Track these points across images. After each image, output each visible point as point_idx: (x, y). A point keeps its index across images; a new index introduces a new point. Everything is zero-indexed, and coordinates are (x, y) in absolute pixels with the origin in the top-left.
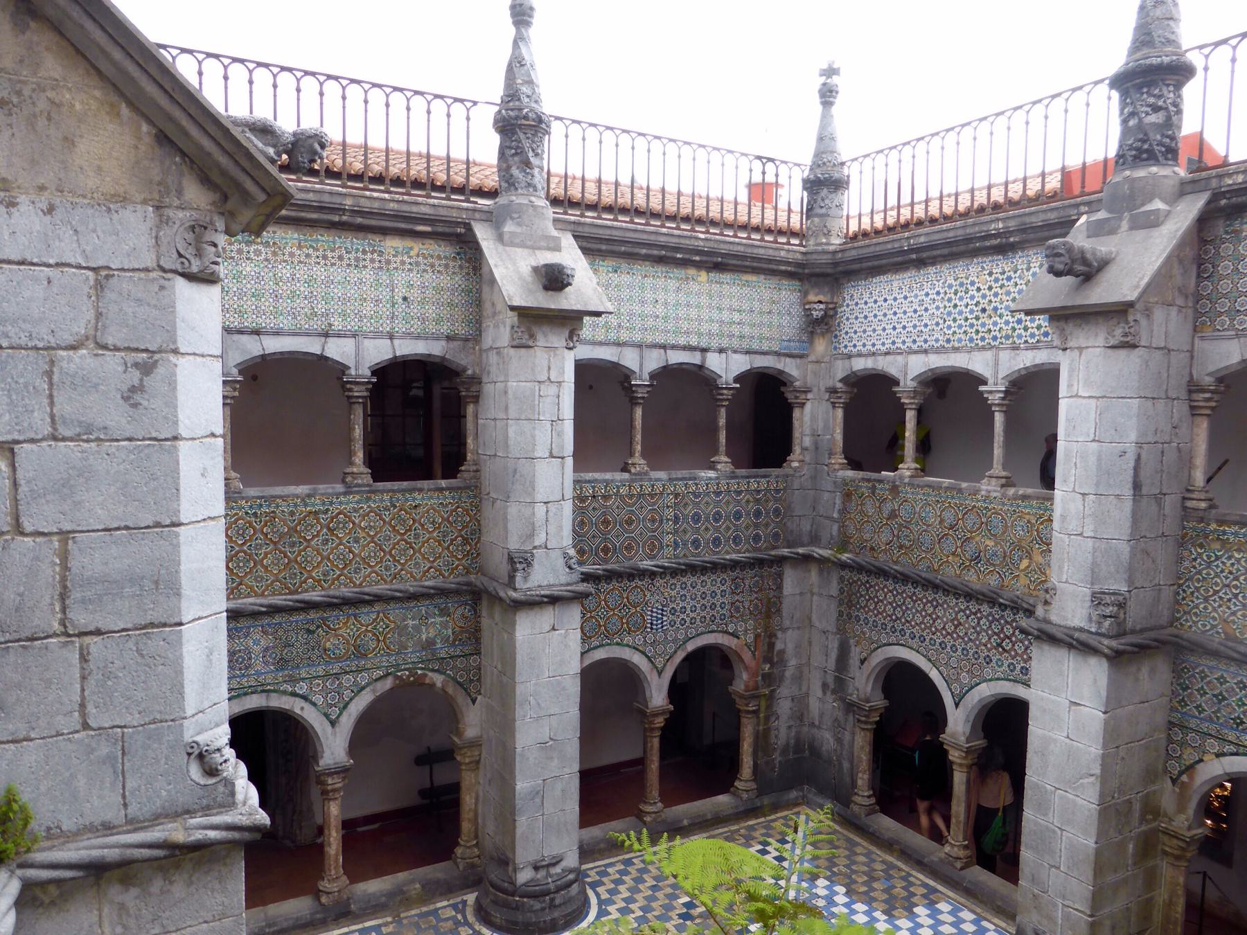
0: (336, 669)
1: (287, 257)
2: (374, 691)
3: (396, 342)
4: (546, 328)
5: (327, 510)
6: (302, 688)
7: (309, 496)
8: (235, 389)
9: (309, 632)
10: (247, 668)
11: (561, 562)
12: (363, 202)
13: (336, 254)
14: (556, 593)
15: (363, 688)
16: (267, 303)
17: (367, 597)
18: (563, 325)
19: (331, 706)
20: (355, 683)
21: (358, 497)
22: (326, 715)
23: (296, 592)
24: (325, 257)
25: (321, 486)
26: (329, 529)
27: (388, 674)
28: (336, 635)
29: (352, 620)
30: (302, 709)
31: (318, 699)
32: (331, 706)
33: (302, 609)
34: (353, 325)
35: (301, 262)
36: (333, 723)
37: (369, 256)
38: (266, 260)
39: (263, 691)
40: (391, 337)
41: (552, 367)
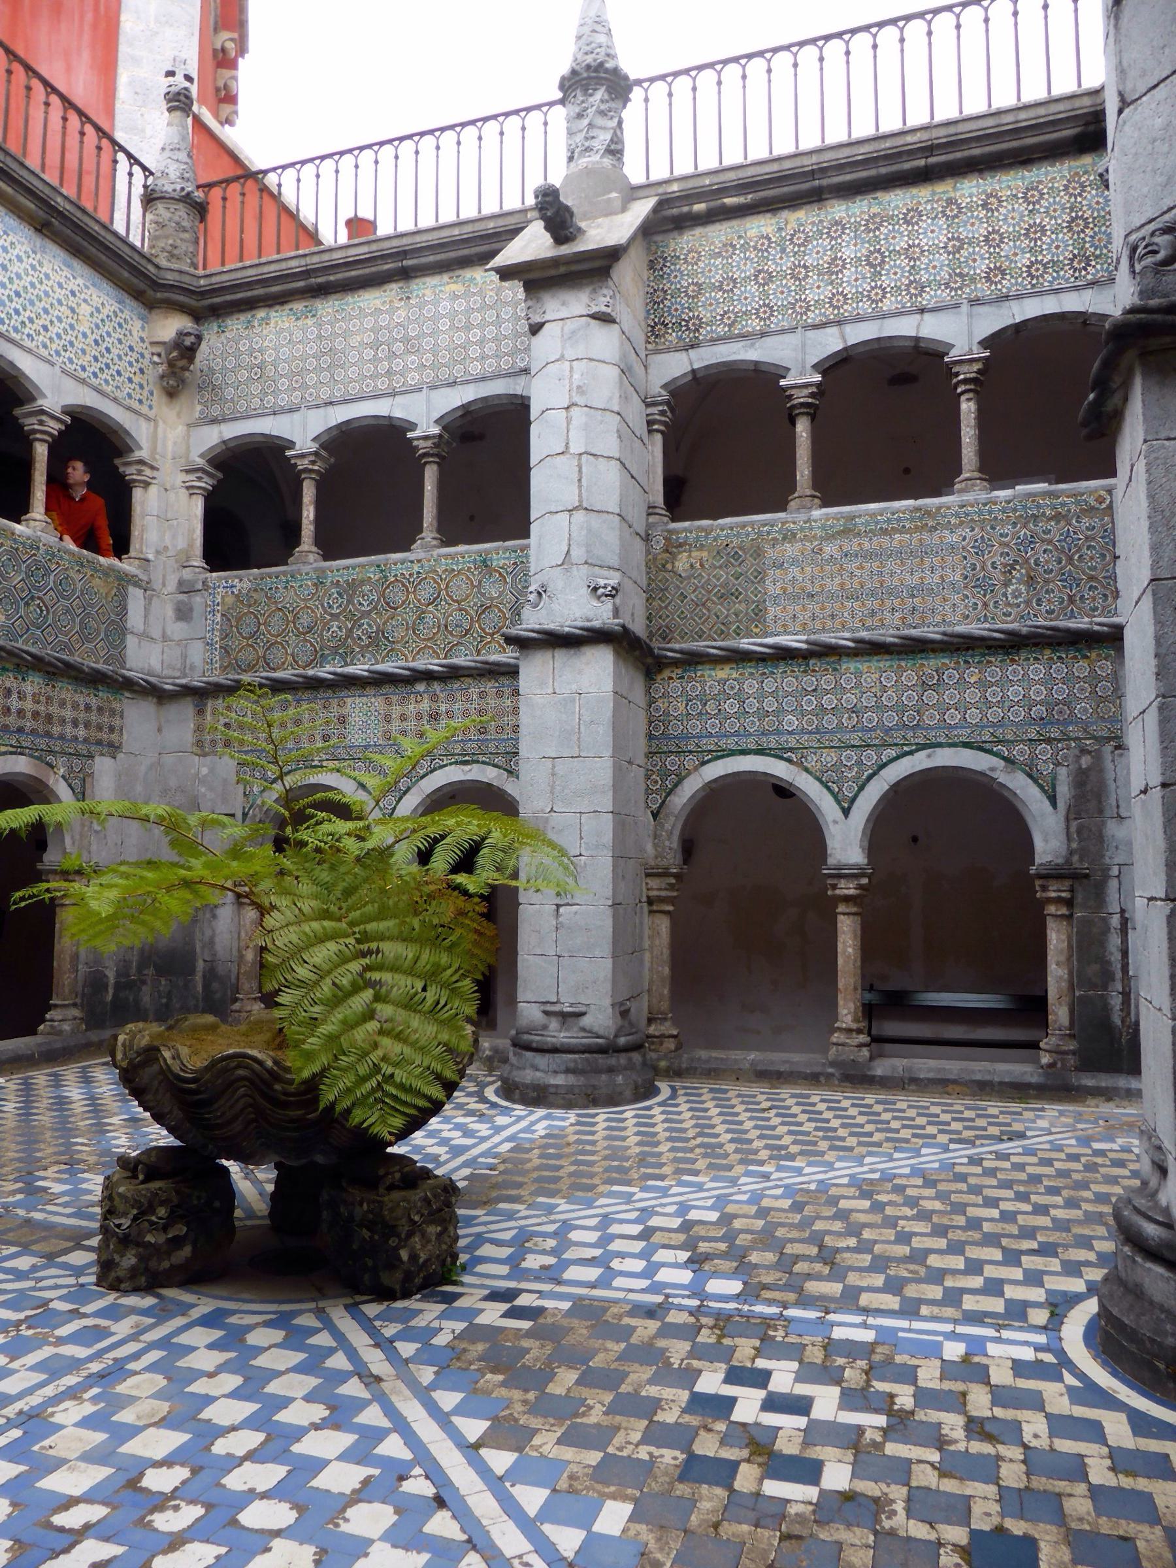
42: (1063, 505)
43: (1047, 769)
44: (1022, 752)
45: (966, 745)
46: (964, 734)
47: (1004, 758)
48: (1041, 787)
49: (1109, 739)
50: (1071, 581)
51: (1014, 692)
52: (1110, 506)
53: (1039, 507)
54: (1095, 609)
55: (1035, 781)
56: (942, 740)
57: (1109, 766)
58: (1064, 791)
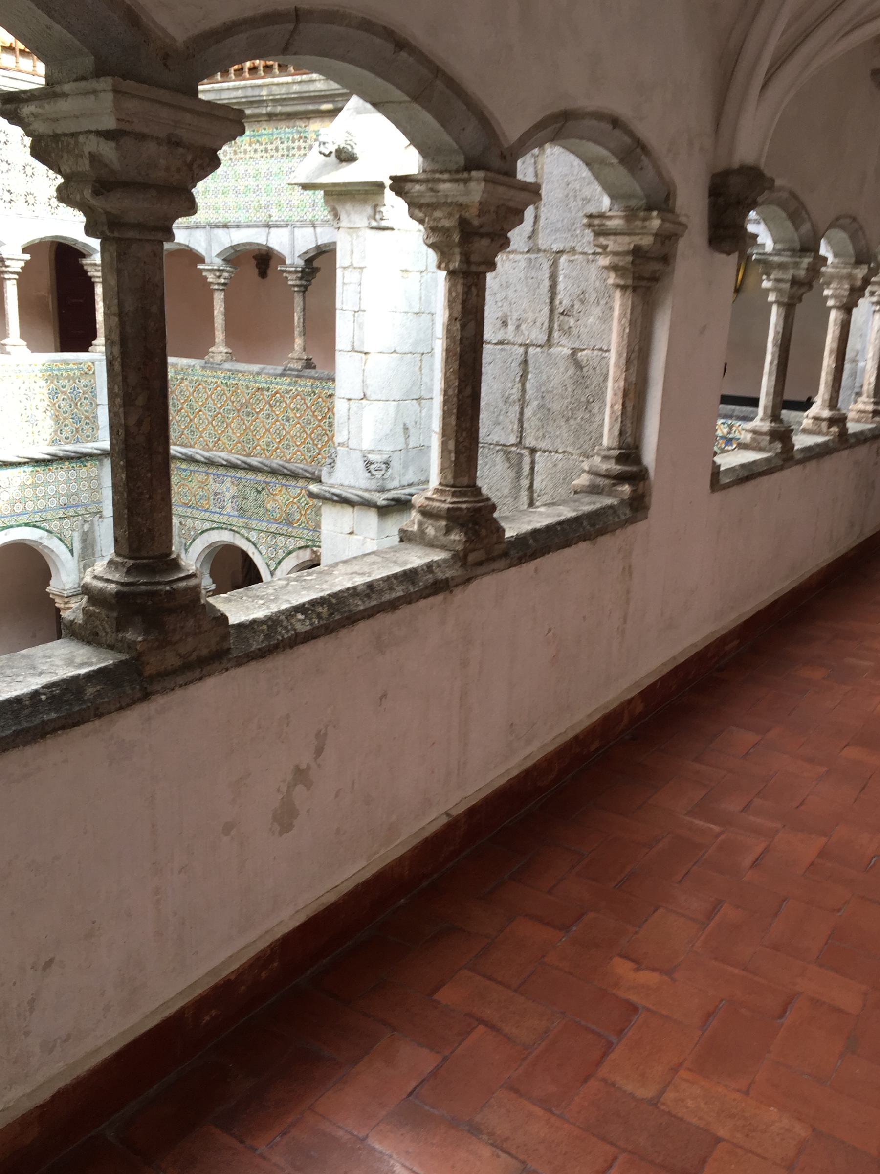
0: (273, 528)
1: (242, 155)
2: (298, 557)
3: (319, 230)
4: (348, 207)
5: (269, 389)
6: (253, 536)
7: (258, 374)
8: (219, 277)
9: (259, 492)
10: (223, 508)
11: (361, 465)
12: (276, 90)
13: (273, 146)
14: (344, 494)
15: (290, 553)
16: (231, 199)
17: (286, 471)
18: (365, 201)
19: (271, 559)
20: (285, 546)
21: (289, 380)
22: (268, 566)
23: (248, 455)
24: (266, 150)
25: (269, 367)
26: (270, 405)
27: (307, 547)
28: (275, 500)
29: (284, 490)
30: (253, 553)
31: (262, 548)
32: (271, 559)
33: (244, 469)
34: (285, 215)
35: (251, 158)
36: (272, 574)
37: (297, 144)
38: (231, 159)
39: (231, 530)
40: (314, 227)
41: (355, 251)
42: (72, 369)
43: (68, 534)
44: (56, 526)
45: (27, 525)
46: (25, 519)
47: (47, 531)
48: (66, 545)
49: (96, 513)
50: (76, 419)
51: (51, 490)
52: (94, 373)
53: (59, 370)
54: (88, 437)
55: (63, 542)
56: (13, 523)
57: (96, 528)
58: (77, 546)
